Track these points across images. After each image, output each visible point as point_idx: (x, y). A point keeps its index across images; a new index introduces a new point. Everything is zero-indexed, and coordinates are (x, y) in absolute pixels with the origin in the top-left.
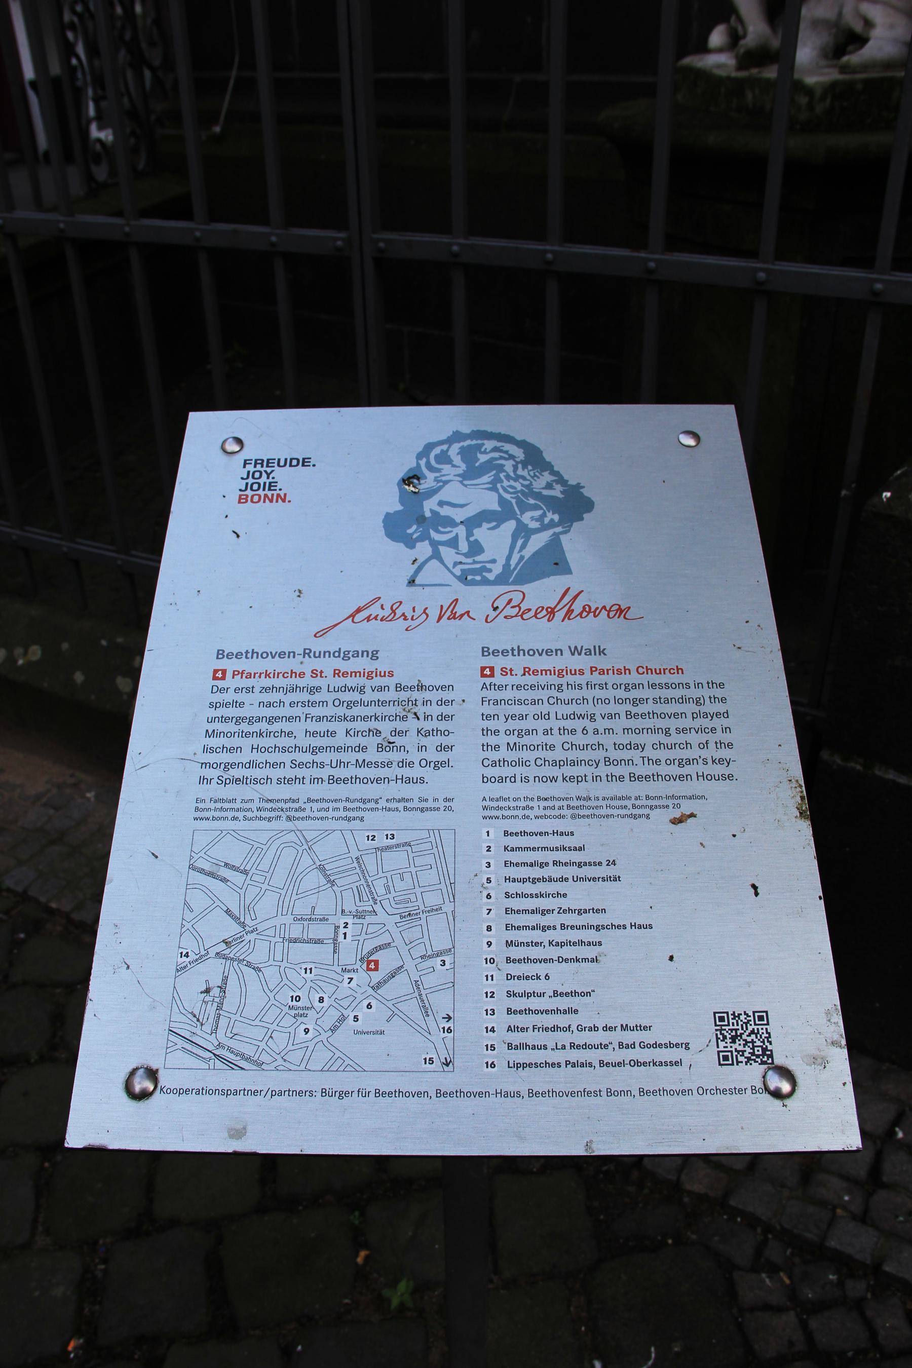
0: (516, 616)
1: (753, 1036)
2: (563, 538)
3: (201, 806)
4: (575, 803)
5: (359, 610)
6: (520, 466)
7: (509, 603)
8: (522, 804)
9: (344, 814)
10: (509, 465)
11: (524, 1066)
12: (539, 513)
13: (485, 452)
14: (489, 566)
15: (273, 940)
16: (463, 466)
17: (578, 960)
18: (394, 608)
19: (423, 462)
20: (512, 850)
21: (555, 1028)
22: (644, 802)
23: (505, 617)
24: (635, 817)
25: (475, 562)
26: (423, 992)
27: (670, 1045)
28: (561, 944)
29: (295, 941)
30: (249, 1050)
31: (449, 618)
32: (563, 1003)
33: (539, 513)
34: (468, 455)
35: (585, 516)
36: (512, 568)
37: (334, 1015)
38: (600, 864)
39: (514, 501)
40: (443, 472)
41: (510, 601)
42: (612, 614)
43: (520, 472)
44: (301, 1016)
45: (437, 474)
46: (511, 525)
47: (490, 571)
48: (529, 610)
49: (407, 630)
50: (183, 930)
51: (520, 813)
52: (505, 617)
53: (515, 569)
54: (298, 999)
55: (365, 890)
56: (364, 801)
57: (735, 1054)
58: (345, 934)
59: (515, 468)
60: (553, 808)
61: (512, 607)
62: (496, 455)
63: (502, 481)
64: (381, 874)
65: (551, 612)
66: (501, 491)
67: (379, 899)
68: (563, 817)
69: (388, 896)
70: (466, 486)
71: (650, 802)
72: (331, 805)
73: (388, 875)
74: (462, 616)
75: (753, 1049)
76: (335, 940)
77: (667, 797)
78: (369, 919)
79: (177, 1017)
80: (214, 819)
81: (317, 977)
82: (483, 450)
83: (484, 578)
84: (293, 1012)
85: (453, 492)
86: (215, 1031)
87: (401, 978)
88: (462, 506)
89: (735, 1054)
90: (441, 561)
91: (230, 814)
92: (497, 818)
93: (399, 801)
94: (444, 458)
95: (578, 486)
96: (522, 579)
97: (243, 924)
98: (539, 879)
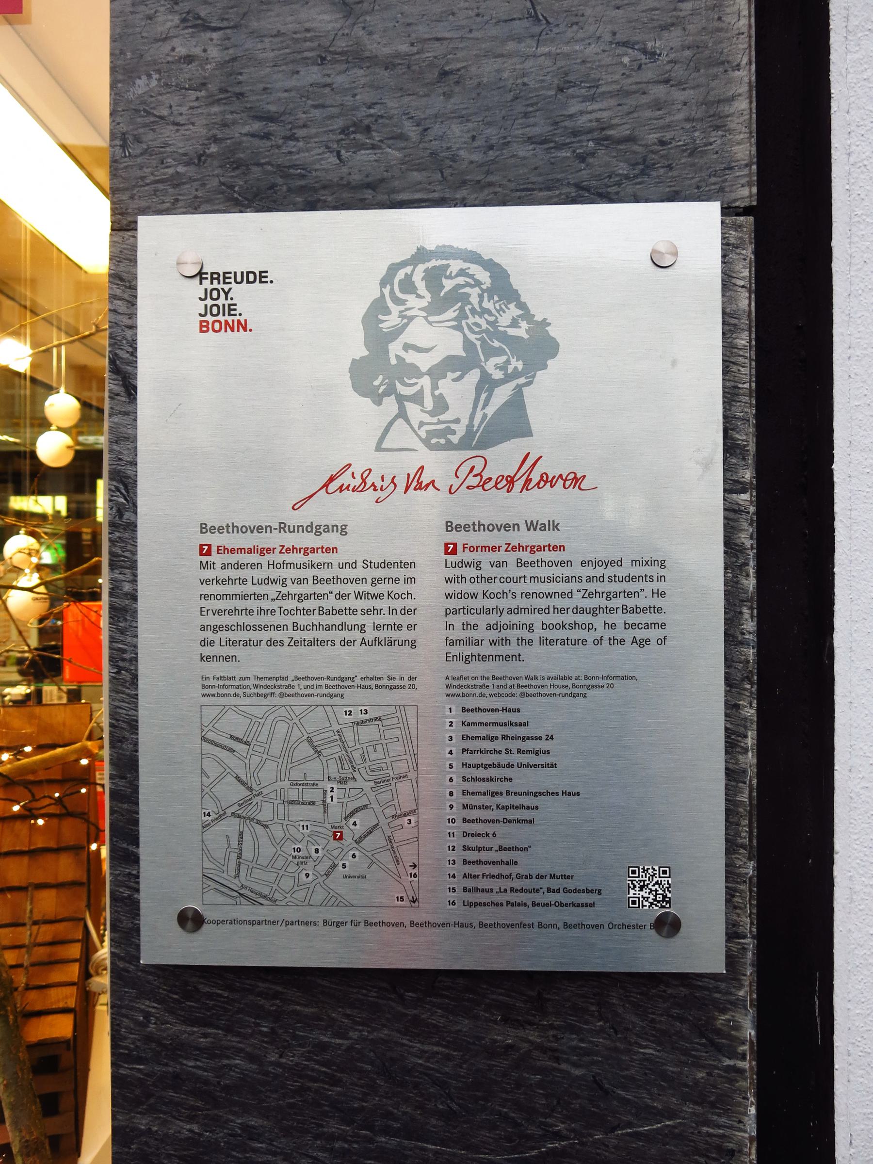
0: (478, 486)
1: (657, 886)
2: (525, 390)
3: (207, 683)
4: (524, 682)
5: (332, 479)
6: (486, 295)
7: (471, 471)
8: (479, 682)
9: (327, 691)
10: (474, 293)
11: (476, 904)
12: (504, 358)
13: (450, 277)
14: (453, 426)
15: (276, 802)
16: (428, 297)
17: (519, 822)
18: (365, 476)
19: (387, 291)
20: (469, 724)
21: (500, 876)
22: (583, 682)
23: (468, 488)
24: (574, 696)
25: (440, 422)
26: (395, 845)
27: (587, 891)
28: (506, 808)
29: (292, 802)
30: (266, 891)
31: (415, 489)
32: (505, 856)
33: (504, 358)
34: (434, 278)
35: (549, 362)
36: (475, 429)
37: (327, 864)
38: (540, 738)
39: (478, 343)
40: (409, 305)
41: (473, 467)
42: (568, 483)
43: (487, 304)
44: (302, 863)
45: (402, 308)
46: (474, 376)
47: (454, 432)
48: (490, 479)
49: (377, 502)
50: (204, 793)
51: (478, 691)
52: (468, 488)
53: (478, 430)
54: (299, 850)
55: (346, 759)
56: (342, 679)
57: (641, 899)
58: (332, 797)
59: (481, 297)
60: (505, 687)
61: (474, 476)
62: (461, 280)
63: (467, 318)
64: (358, 746)
65: (511, 481)
66: (466, 331)
67: (357, 767)
68: (514, 695)
69: (367, 765)
70: (430, 323)
71: (588, 682)
72: (315, 682)
73: (364, 746)
74: (427, 486)
75: (656, 896)
76: (324, 802)
77: (603, 678)
78: (351, 784)
79: (207, 864)
80: (219, 695)
81: (313, 833)
82: (448, 273)
83: (449, 442)
84: (296, 861)
85: (420, 332)
86: (237, 876)
87: (377, 833)
88: (427, 350)
89: (641, 899)
90: (407, 421)
91: (232, 691)
92: (458, 695)
93: (372, 679)
94: (408, 286)
95: (545, 323)
96: (484, 444)
97: (250, 789)
98: (490, 765)
